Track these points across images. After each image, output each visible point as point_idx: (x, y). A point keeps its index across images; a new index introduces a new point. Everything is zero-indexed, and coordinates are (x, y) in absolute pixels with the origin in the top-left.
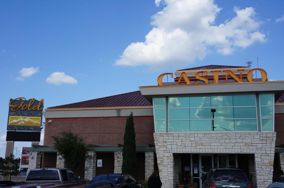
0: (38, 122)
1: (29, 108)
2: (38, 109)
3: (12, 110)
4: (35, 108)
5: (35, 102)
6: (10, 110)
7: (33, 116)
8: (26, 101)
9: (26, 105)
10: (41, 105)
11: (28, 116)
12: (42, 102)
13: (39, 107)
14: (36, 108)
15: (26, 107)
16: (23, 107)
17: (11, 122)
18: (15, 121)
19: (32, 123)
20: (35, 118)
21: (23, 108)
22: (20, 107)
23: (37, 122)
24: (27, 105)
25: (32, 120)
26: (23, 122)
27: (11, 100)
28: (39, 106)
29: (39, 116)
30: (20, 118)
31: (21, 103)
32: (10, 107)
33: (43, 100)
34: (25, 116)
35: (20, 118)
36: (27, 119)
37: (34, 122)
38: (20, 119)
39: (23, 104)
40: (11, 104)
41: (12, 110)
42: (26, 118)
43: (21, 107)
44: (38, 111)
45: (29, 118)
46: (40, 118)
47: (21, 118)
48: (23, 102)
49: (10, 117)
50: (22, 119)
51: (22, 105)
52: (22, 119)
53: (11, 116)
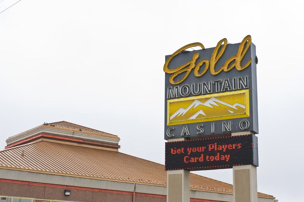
0: (240, 106)
1: (215, 68)
2: (239, 68)
3: (172, 82)
4: (228, 68)
5: (225, 49)
6: (168, 85)
7: (226, 90)
8: (204, 49)
9: (205, 63)
10: (244, 53)
11: (214, 92)
12: (246, 43)
13: (241, 62)
14: (232, 67)
15: (207, 68)
16: (198, 68)
17: (172, 118)
18: (182, 111)
19: (226, 110)
20: (226, 96)
21: (199, 71)
22: (189, 70)
23: (236, 105)
24: (207, 62)
25: (224, 103)
26: (201, 112)
27: (167, 57)
28: (239, 59)
29: (243, 89)
30: (193, 100)
31: (192, 60)
32: (168, 76)
33: (249, 37)
34: (207, 94)
35: (193, 100)
36: (212, 101)
37: (230, 106)
38: (194, 103)
39: (197, 60)
40: (168, 67)
41: (172, 82)
42: (207, 99)
43: (193, 69)
44: (227, 72)
45: (216, 98)
46: (247, 92)
47: (196, 102)
48: (197, 56)
49: (169, 101)
50: (197, 103)
51: (195, 64)
52: (197, 103)
53: (171, 99)
